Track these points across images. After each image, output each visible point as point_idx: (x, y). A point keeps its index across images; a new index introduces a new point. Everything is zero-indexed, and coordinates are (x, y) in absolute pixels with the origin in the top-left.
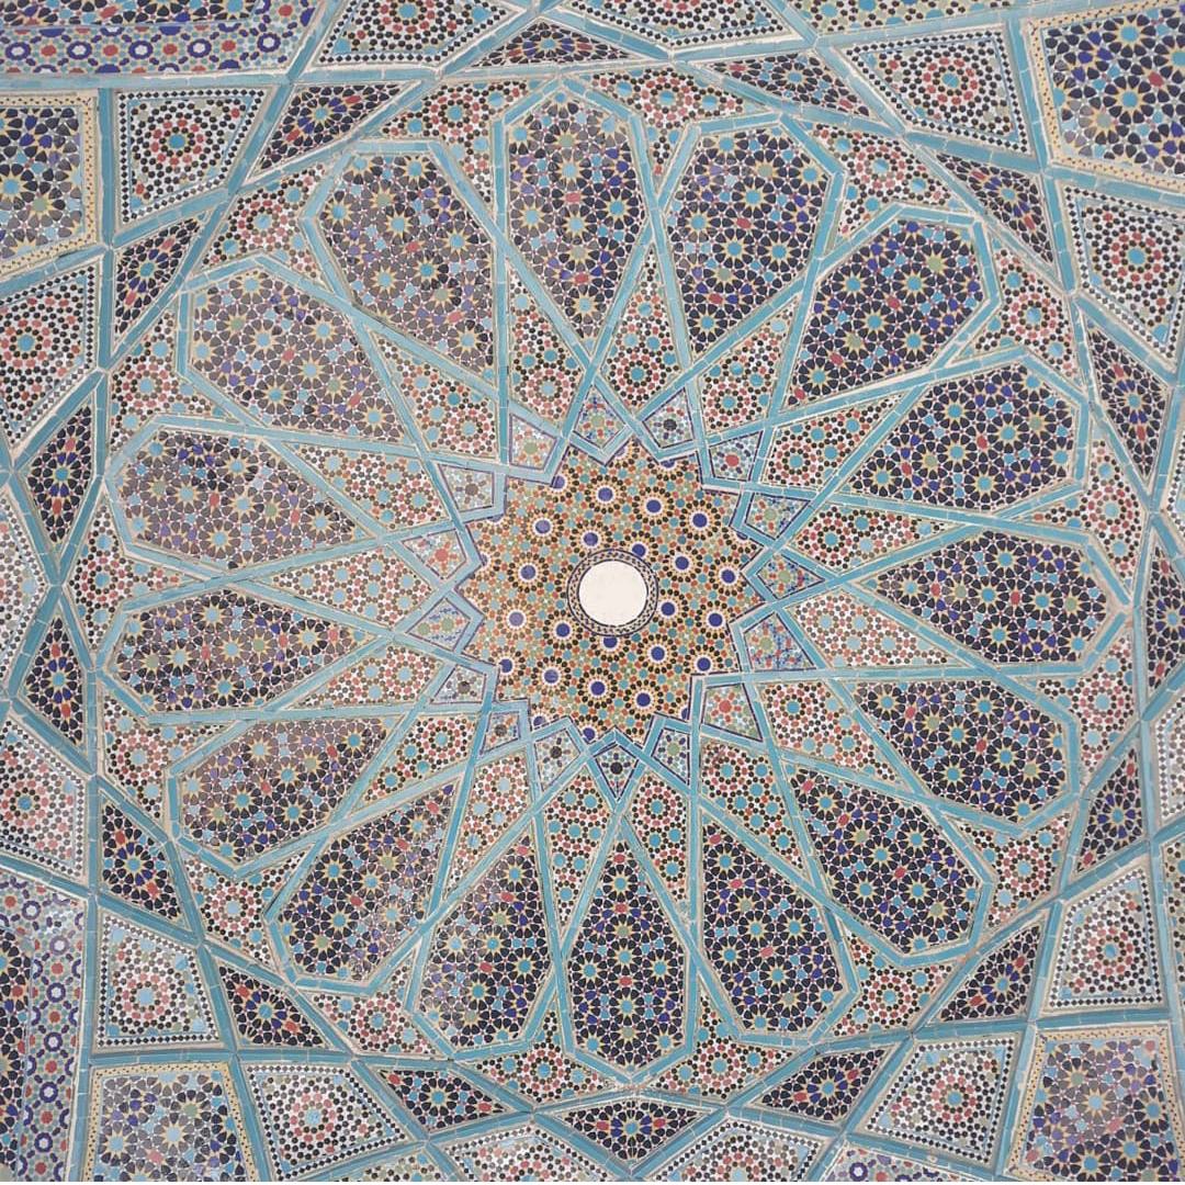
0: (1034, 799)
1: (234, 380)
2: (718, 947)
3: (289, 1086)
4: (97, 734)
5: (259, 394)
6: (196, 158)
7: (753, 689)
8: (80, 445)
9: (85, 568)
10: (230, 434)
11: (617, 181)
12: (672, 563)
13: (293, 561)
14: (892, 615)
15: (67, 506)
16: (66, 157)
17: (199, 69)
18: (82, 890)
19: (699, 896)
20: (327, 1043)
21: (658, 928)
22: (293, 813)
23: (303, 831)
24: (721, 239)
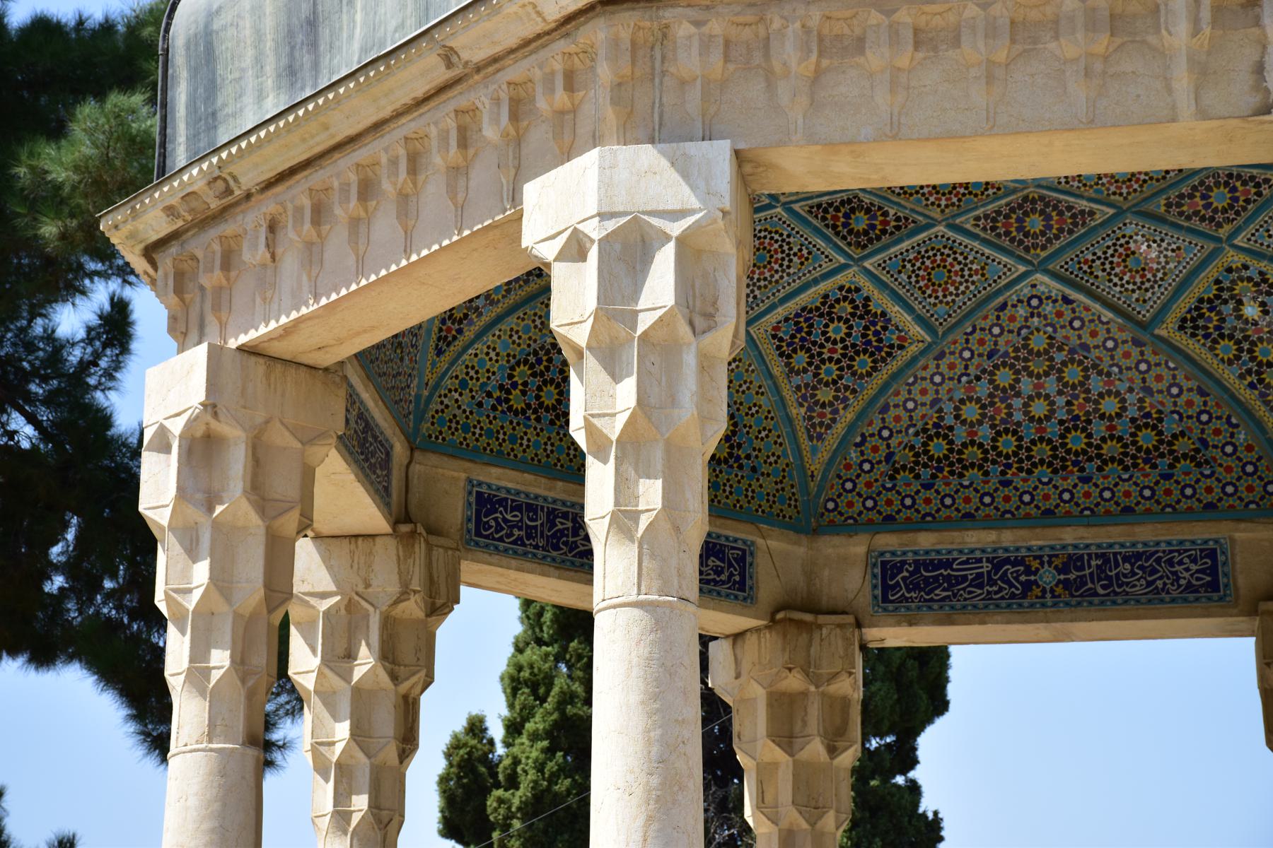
17: (1087, 309)
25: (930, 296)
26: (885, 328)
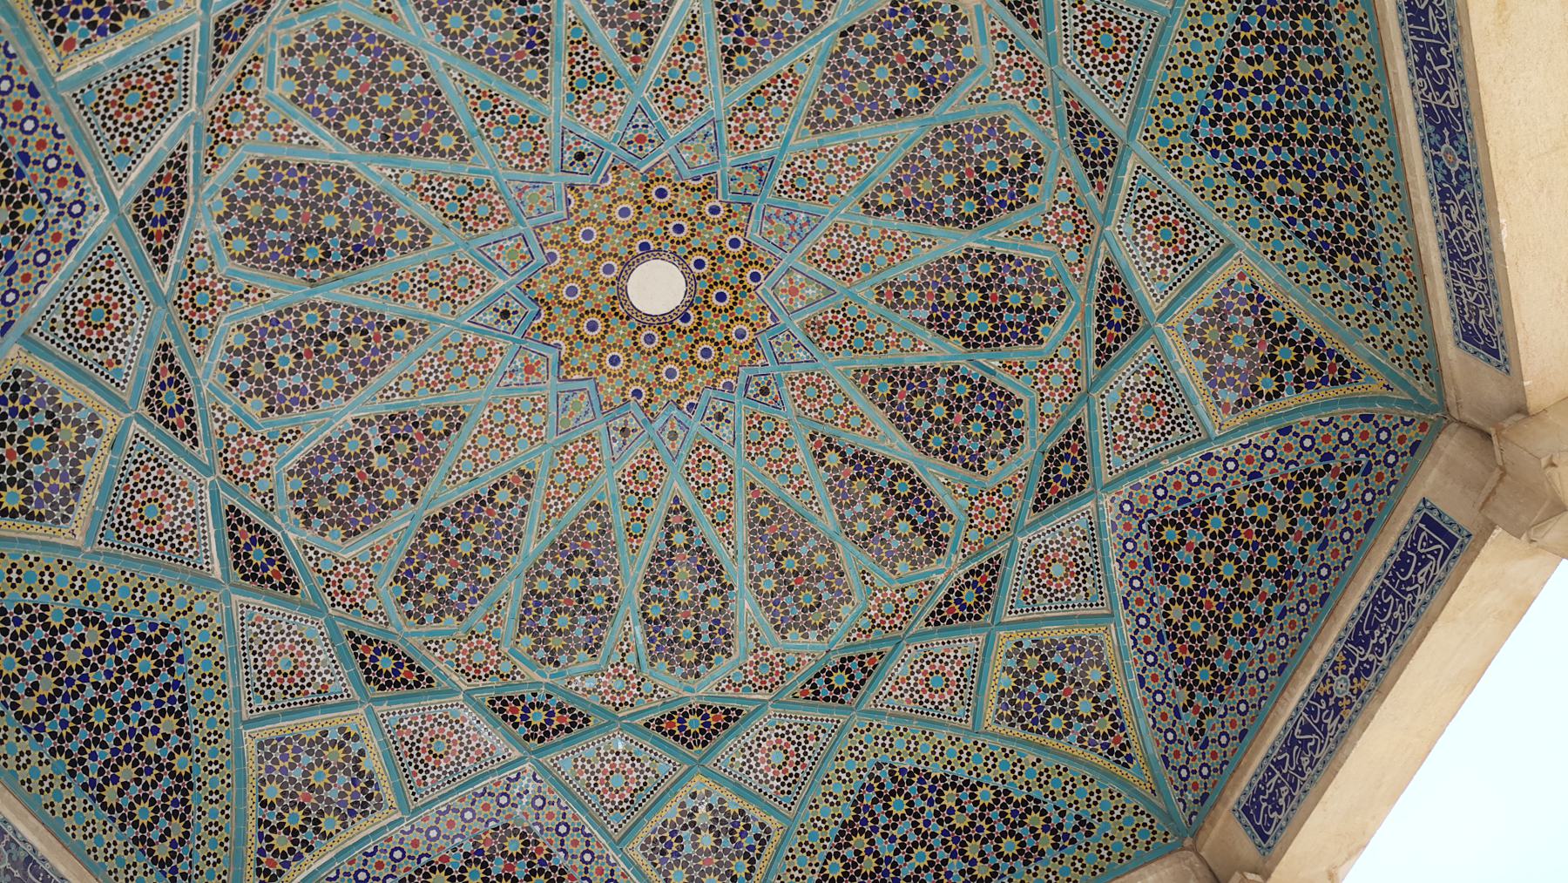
0: (1034, 177)
1: (294, 401)
2: (925, 443)
3: (747, 752)
4: (439, 667)
5: (318, 394)
6: (119, 311)
7: (800, 265)
8: (250, 529)
9: (331, 589)
10: (327, 433)
11: (377, 50)
12: (673, 235)
13: (447, 462)
14: (834, 141)
15: (282, 568)
16: (47, 395)
17: (57, 268)
18: (520, 760)
19: (887, 422)
20: (747, 708)
21: (880, 465)
22: (599, 601)
23: (615, 605)
24: (481, 17)
25: (114, 86)
26: (92, 25)
